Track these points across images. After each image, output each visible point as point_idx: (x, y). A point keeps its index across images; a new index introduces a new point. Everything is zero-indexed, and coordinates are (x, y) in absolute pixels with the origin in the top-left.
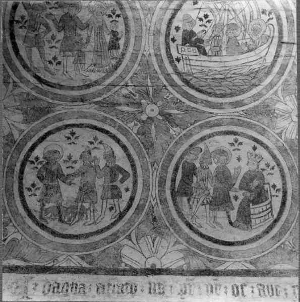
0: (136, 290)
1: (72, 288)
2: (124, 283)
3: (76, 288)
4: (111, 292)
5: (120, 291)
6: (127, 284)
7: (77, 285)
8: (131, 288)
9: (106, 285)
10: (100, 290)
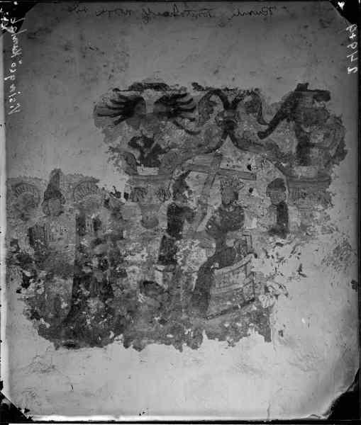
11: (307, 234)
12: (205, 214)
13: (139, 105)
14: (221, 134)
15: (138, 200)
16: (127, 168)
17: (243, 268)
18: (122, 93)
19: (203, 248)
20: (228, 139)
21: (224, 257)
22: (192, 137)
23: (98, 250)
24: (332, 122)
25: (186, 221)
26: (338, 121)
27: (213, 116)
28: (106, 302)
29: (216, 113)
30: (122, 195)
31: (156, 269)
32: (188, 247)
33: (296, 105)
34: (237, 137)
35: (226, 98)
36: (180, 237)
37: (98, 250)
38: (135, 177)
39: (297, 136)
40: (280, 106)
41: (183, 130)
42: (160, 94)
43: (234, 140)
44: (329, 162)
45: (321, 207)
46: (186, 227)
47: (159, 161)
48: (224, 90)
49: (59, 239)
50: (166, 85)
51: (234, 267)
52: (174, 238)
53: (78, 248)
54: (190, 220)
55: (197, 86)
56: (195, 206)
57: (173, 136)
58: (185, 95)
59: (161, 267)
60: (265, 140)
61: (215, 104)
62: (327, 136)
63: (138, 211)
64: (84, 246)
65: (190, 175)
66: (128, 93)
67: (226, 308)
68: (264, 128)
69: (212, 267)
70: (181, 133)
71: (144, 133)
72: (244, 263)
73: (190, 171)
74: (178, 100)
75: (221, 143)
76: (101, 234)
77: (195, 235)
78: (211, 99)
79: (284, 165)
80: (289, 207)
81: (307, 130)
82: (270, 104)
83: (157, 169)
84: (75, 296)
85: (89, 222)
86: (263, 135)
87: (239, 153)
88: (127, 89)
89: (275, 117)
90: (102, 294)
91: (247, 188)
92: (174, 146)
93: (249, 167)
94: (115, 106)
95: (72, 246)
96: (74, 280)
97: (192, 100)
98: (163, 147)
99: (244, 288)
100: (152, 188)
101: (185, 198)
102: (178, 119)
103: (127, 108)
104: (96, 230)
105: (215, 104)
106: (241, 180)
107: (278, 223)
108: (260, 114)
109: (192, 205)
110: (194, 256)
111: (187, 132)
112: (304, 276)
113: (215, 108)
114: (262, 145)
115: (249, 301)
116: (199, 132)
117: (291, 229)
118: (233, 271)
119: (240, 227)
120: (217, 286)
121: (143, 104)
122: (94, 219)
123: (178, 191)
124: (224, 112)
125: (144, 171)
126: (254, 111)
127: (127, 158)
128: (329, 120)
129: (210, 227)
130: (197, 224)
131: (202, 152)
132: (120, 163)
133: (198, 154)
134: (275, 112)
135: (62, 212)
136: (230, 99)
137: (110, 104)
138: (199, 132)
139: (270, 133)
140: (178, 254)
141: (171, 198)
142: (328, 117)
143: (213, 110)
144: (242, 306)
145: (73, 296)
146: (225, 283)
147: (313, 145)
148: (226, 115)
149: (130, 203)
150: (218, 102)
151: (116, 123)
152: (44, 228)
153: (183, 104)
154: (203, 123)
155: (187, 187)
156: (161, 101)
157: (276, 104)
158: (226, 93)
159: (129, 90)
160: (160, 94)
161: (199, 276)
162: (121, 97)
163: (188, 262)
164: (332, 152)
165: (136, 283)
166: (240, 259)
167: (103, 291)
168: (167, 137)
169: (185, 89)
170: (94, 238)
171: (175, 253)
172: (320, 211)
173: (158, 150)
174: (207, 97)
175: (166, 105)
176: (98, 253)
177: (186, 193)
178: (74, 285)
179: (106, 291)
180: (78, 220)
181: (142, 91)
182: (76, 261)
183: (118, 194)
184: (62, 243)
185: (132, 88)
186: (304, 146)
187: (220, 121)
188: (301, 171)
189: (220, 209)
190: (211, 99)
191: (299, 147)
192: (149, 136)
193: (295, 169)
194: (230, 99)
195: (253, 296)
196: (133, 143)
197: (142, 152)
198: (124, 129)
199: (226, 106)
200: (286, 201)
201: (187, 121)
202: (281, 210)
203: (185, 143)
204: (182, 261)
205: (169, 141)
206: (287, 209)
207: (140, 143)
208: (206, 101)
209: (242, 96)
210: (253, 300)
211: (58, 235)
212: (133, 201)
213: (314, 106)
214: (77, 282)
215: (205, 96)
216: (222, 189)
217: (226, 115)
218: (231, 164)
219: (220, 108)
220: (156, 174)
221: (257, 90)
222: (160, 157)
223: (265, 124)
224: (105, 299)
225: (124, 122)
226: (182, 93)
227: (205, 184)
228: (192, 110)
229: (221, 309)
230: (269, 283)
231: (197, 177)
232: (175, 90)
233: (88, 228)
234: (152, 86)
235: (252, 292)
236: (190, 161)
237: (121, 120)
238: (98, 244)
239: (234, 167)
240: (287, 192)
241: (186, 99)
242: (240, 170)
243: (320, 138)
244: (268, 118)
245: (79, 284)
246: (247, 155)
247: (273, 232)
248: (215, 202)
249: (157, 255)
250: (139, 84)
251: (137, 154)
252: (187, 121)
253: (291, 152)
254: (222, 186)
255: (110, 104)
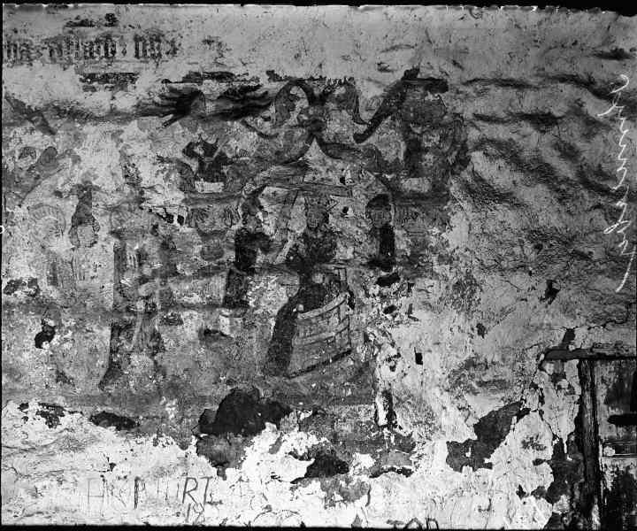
0: (114, 52)
1: (9, 51)
2: (93, 40)
3: (15, 51)
4: (73, 56)
5: (88, 54)
6: (98, 41)
7: (16, 46)
8: (106, 49)
9: (64, 44)
10: (56, 54)
11: (419, 265)
12: (285, 241)
13: (196, 101)
14: (306, 137)
15: (196, 225)
16: (182, 184)
17: (335, 311)
18: (174, 86)
19: (282, 285)
20: (315, 143)
21: (311, 297)
22: (266, 141)
23: (142, 291)
24: (451, 120)
25: (260, 251)
26: (458, 118)
27: (294, 116)
28: (155, 358)
29: (298, 109)
30: (176, 218)
31: (221, 313)
32: (262, 284)
33: (403, 98)
34: (326, 140)
35: (312, 90)
36: (252, 272)
37: (142, 291)
38: (193, 196)
39: (405, 138)
40: (381, 100)
41: (255, 133)
42: (224, 86)
43: (322, 144)
44: (447, 171)
45: (436, 230)
46: (260, 258)
47: (223, 173)
48: (308, 80)
49: (93, 278)
50: (232, 75)
51: (323, 310)
52: (245, 273)
53: (117, 289)
54: (266, 250)
55: (272, 75)
56: (273, 231)
57: (241, 140)
58: (259, 86)
59: (226, 312)
60: (364, 144)
61: (297, 98)
62: (443, 138)
63: (197, 238)
64: (125, 286)
65: (265, 191)
66: (181, 85)
67: (314, 363)
68: (362, 128)
69: (295, 310)
70: (253, 136)
71: (204, 138)
72: (336, 304)
73: (264, 186)
74: (248, 94)
75: (306, 149)
76: (147, 271)
77: (271, 268)
78: (291, 92)
79: (389, 177)
80: (396, 231)
81: (418, 130)
82: (369, 97)
83: (222, 184)
84: (113, 351)
85: (131, 254)
86: (360, 138)
87: (329, 162)
88: (181, 80)
89: (377, 114)
90: (149, 348)
91: (341, 208)
92: (244, 153)
93: (342, 180)
94: (166, 102)
95: (109, 285)
96: (112, 330)
97: (266, 93)
98: (229, 156)
99: (338, 337)
100: (217, 208)
101: (259, 222)
102: (249, 119)
103: (180, 104)
104: (140, 265)
105: (297, 98)
106: (331, 197)
107: (381, 252)
108: (356, 111)
109: (269, 229)
110: (269, 296)
111: (261, 135)
112: (414, 319)
113: (298, 104)
114: (359, 152)
115: (343, 353)
116: (276, 135)
117: (398, 260)
118: (321, 315)
119: (332, 257)
120: (302, 335)
121: (201, 100)
122: (137, 250)
123: (249, 213)
124: (308, 108)
125: (206, 187)
126: (349, 107)
127: (183, 168)
128: (446, 117)
129: (292, 258)
130: (275, 253)
131: (281, 161)
132: (172, 177)
133: (276, 163)
134: (374, 106)
135: (96, 242)
136: (316, 92)
137: (157, 99)
138: (276, 135)
139: (370, 135)
140: (249, 293)
141: (240, 221)
142: (446, 113)
143: (294, 106)
144: (335, 359)
145: (112, 351)
146: (311, 330)
147: (426, 150)
148: (311, 112)
149: (185, 229)
150: (300, 96)
151: (166, 125)
152: (71, 263)
153: (254, 98)
154: (282, 123)
155: (261, 208)
156: (224, 96)
157: (376, 97)
158: (311, 83)
159: (182, 82)
160: (224, 86)
161: (277, 322)
162: (172, 90)
163: (263, 304)
164: (451, 159)
165: (194, 332)
166: (331, 298)
167: (151, 344)
168: (233, 142)
169: (257, 80)
170: (137, 275)
171: (245, 293)
172: (436, 236)
173: (223, 159)
174: (286, 90)
175: (233, 100)
176: (144, 295)
177: (260, 214)
178: (112, 336)
179: (155, 344)
180: (116, 251)
181: (200, 83)
182: (115, 306)
183: (169, 218)
184: (96, 281)
185: (187, 79)
186: (415, 150)
187: (304, 120)
188: (410, 184)
189: (304, 235)
190: (291, 92)
191: (408, 154)
192: (210, 142)
193: (403, 181)
194: (316, 92)
195: (349, 347)
196: (189, 151)
197: (202, 164)
198: (176, 132)
199: (312, 100)
200: (391, 224)
201: (260, 120)
202: (385, 237)
203: (258, 150)
204: (255, 303)
205: (237, 147)
206: (393, 234)
207: (200, 152)
208: (286, 95)
209: (332, 88)
210: (349, 352)
211: (92, 273)
212: (190, 226)
213: (426, 99)
214: (116, 334)
215: (283, 88)
216: (307, 208)
217: (311, 112)
218: (318, 177)
219: (303, 103)
220: (220, 191)
221: (351, 79)
222: (225, 170)
223: (364, 123)
224: (153, 355)
225: (177, 122)
226: (253, 84)
227: (285, 202)
228: (266, 107)
229: (306, 365)
230: (369, 330)
231: (274, 193)
232: (245, 80)
233: (130, 263)
234: (212, 76)
235: (347, 341)
236: (265, 174)
237: (172, 121)
238: (144, 283)
239: (323, 179)
240: (393, 214)
241: (260, 92)
242: (330, 183)
243: (436, 139)
244: (366, 116)
245: (119, 335)
246: (340, 165)
247: (373, 263)
248: (298, 227)
249: (222, 296)
250: (197, 74)
251: (195, 165)
252: (260, 120)
253: (398, 159)
254: (306, 204)
255: (157, 99)
